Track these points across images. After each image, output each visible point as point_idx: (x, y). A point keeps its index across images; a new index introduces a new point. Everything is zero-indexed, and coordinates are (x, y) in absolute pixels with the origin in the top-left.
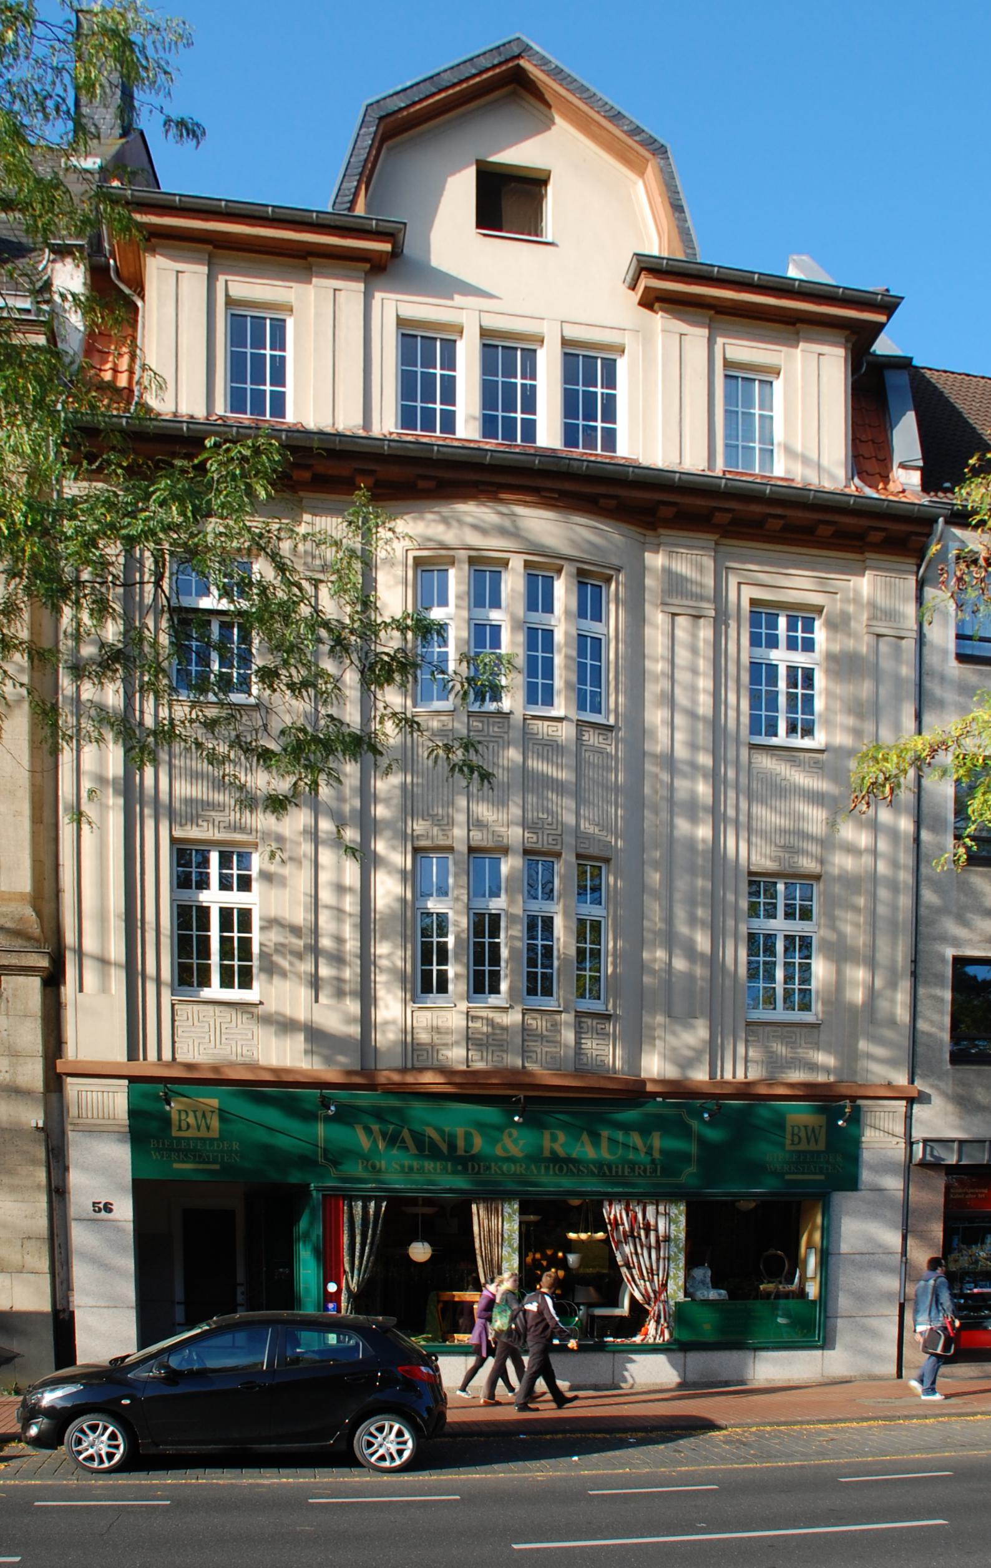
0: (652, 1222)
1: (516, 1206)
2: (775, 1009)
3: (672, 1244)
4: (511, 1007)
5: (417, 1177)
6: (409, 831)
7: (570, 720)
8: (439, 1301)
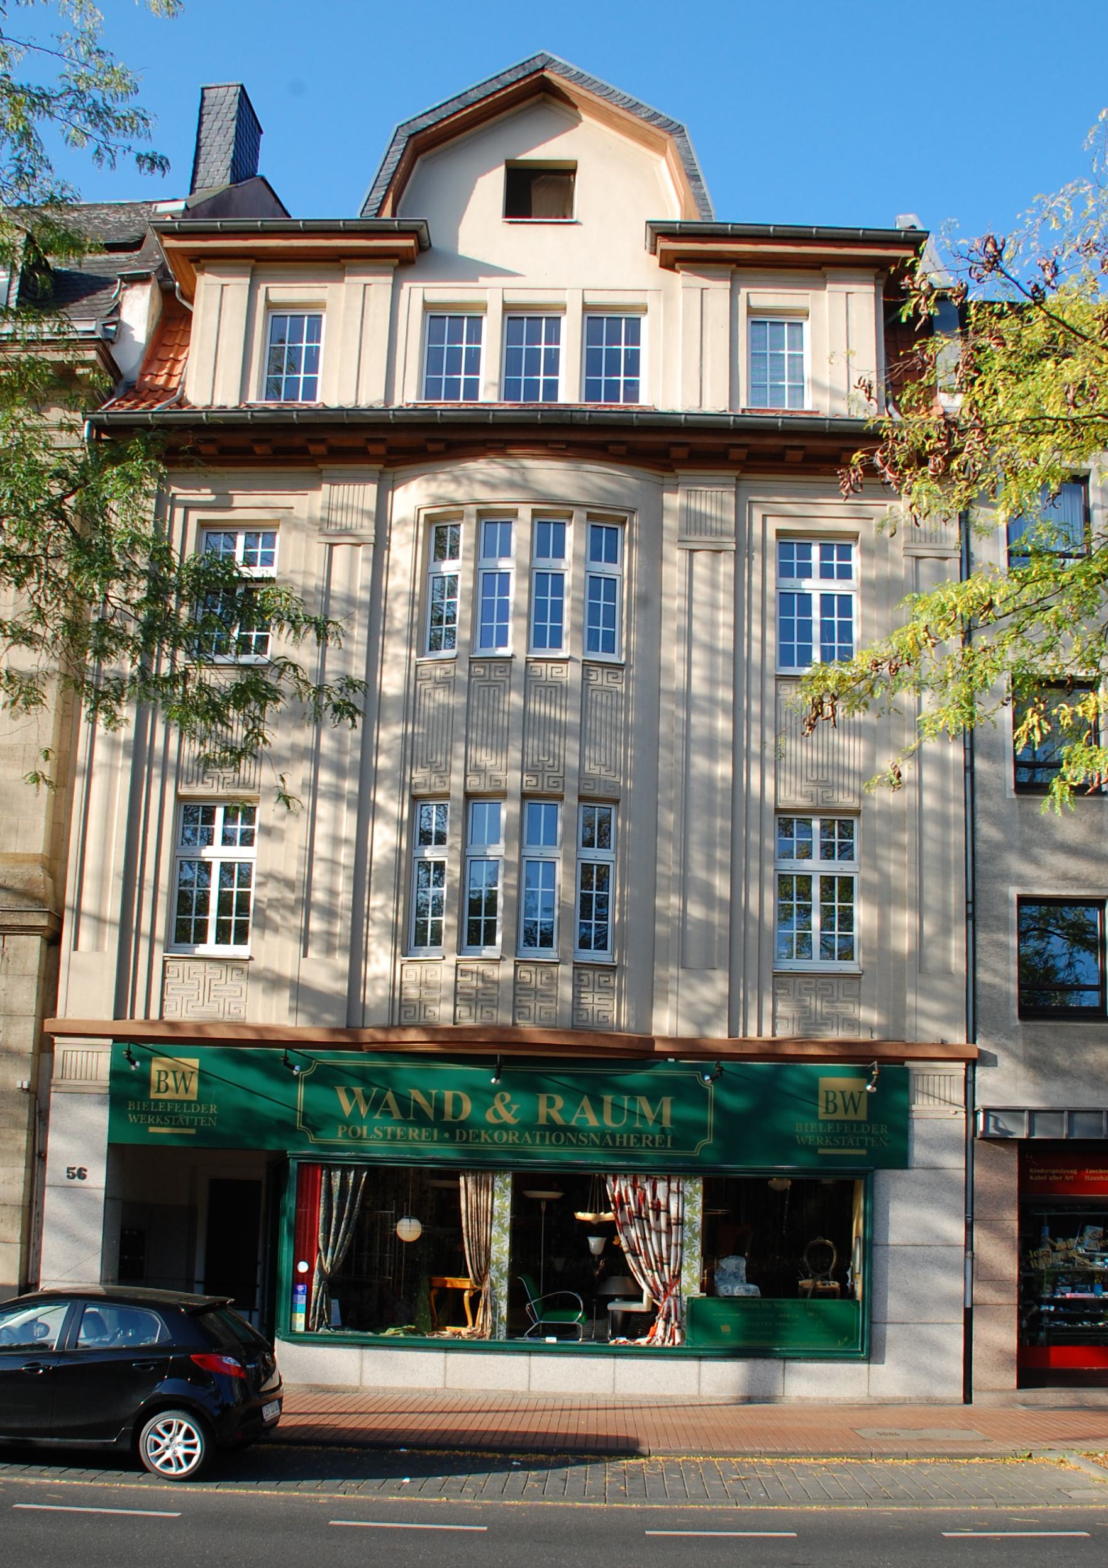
0: (663, 1201)
1: (508, 1180)
2: (811, 958)
3: (686, 1228)
4: (502, 958)
5: (401, 1145)
6: (408, 779)
7: (577, 661)
8: (431, 1288)
